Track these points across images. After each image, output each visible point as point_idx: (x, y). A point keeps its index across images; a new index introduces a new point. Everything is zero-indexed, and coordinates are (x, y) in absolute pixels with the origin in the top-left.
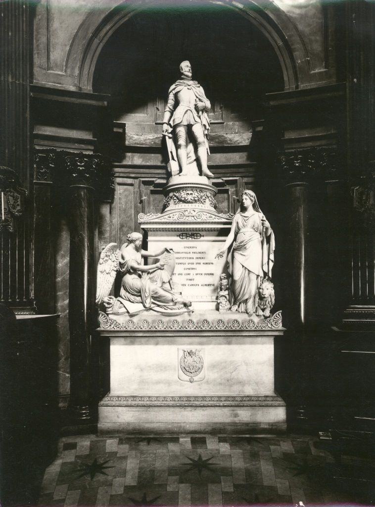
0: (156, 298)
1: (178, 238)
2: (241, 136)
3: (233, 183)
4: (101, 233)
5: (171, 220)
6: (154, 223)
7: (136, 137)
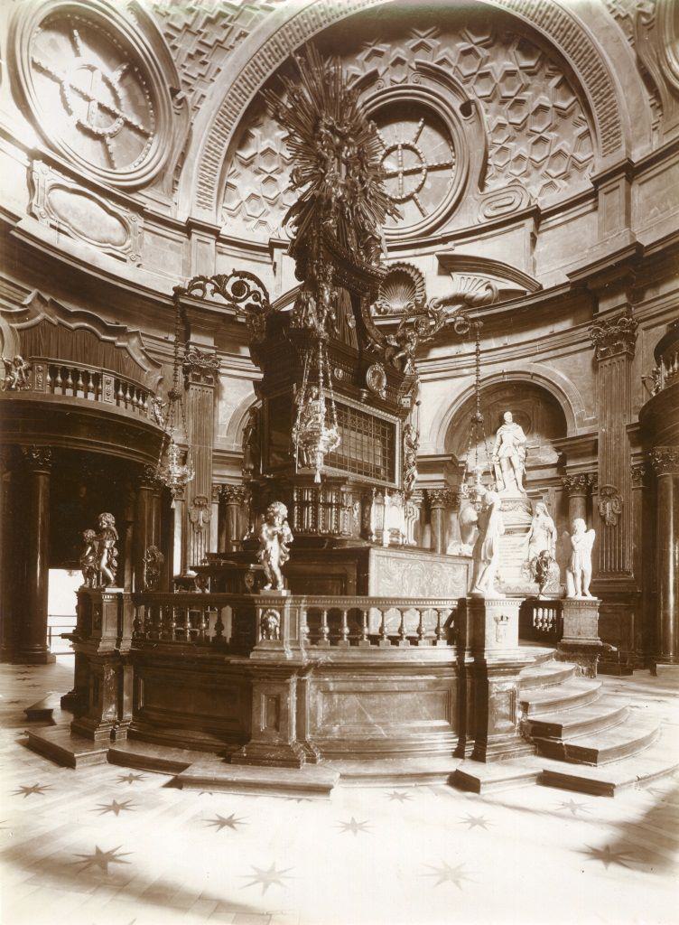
2: (553, 458)
3: (547, 491)
4: (450, 533)
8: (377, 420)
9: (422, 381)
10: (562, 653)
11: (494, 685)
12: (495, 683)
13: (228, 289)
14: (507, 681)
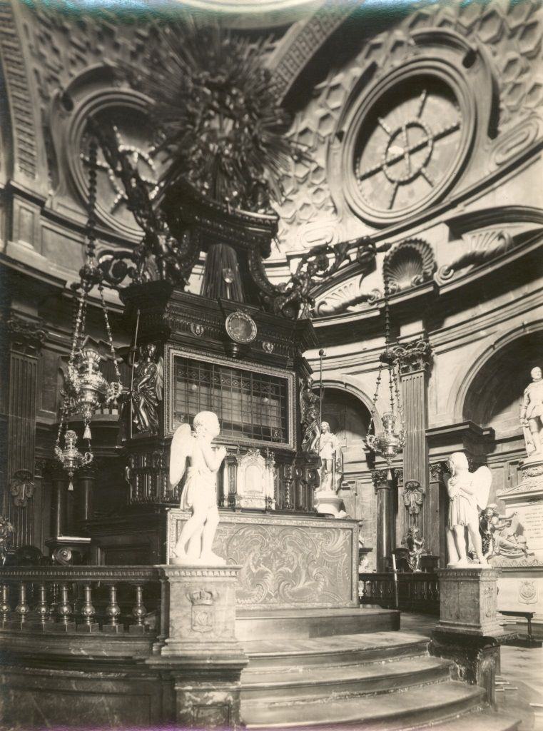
0: (503, 546)
1: (528, 504)
5: (520, 491)
6: (507, 495)
7: (503, 432)
8: (239, 372)
9: (438, 353)
10: (436, 644)
11: (188, 694)
12: (188, 691)
13: (110, 273)
14: (218, 690)
